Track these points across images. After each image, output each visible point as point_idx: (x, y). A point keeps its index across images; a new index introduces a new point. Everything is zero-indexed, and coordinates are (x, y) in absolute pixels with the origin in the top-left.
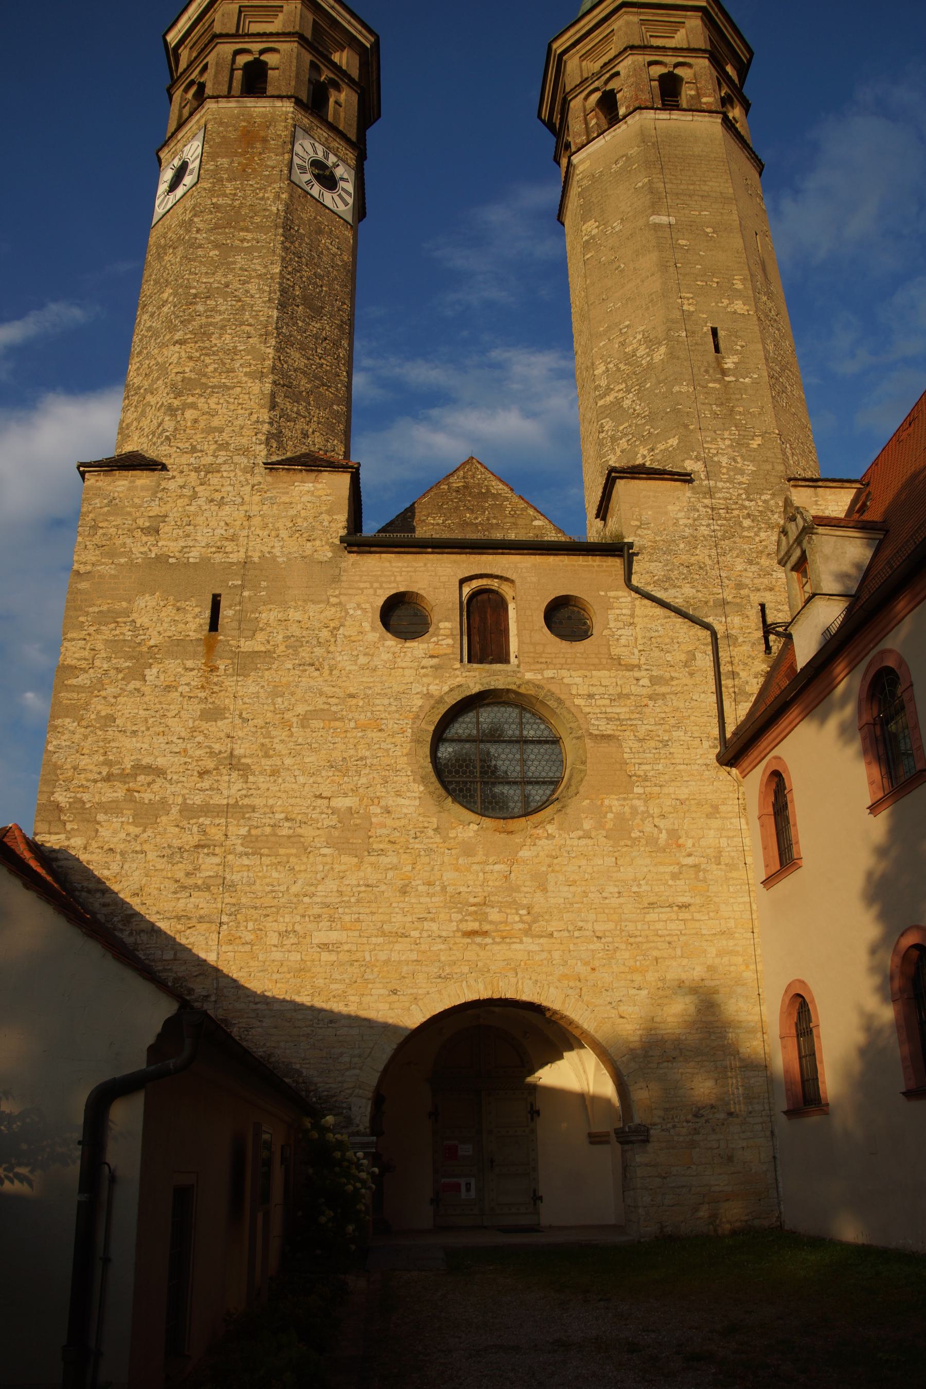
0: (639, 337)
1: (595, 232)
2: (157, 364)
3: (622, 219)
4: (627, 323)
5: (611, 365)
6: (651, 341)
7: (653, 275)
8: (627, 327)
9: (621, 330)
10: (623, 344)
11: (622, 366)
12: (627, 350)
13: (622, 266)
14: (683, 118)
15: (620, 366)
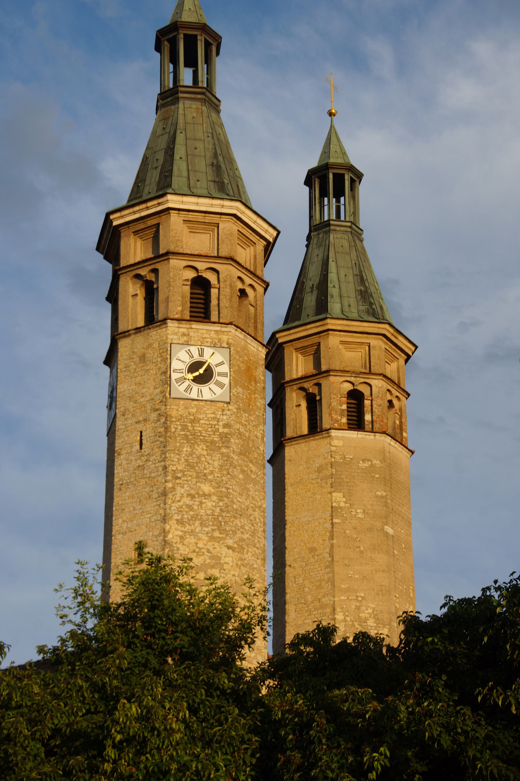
0: (370, 611)
1: (342, 504)
2: (208, 551)
3: (364, 511)
4: (362, 595)
5: (348, 619)
6: (378, 619)
7: (383, 571)
8: (362, 597)
9: (357, 597)
10: (358, 608)
11: (356, 624)
12: (361, 615)
13: (362, 549)
14: (399, 448)
15: (355, 623)
